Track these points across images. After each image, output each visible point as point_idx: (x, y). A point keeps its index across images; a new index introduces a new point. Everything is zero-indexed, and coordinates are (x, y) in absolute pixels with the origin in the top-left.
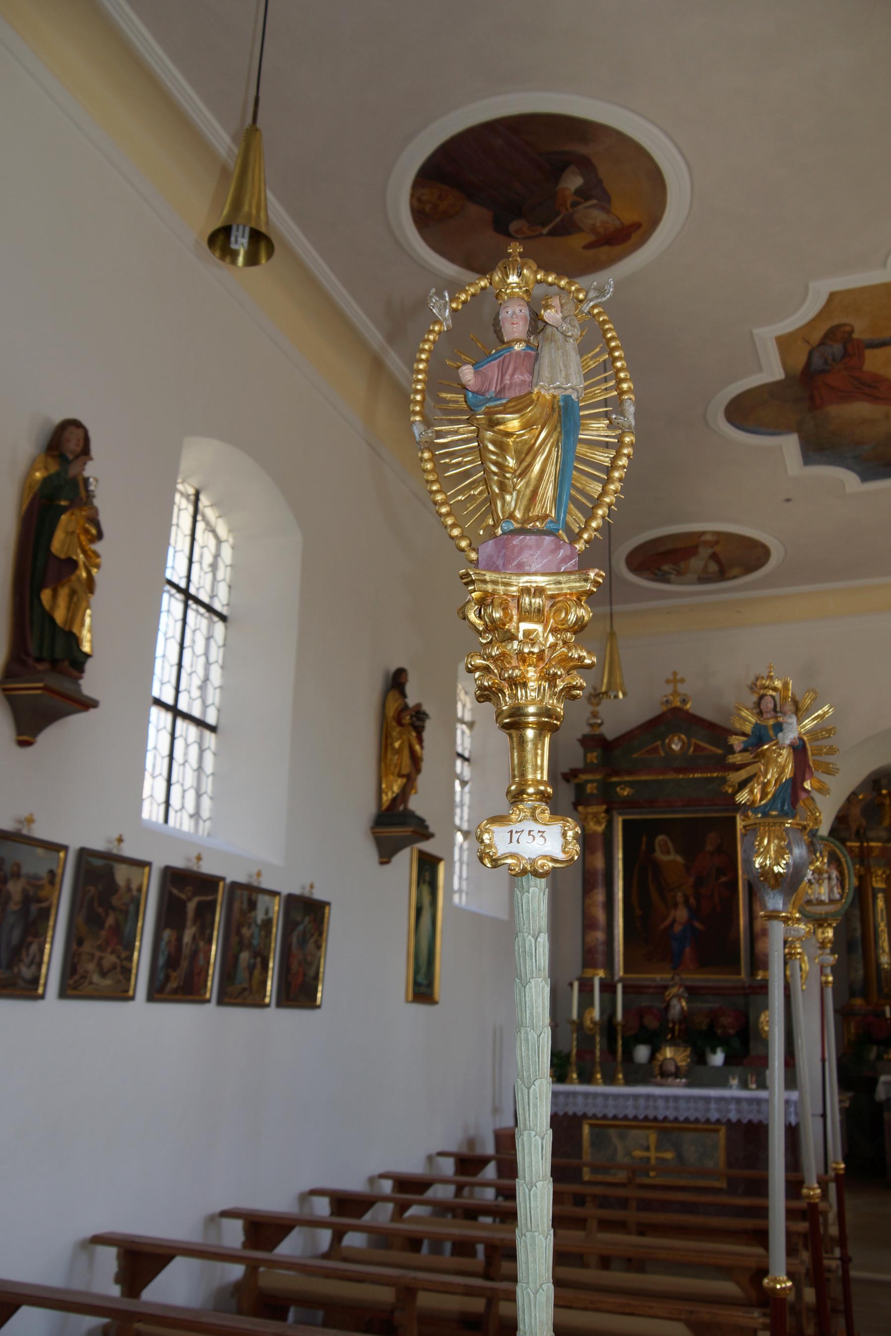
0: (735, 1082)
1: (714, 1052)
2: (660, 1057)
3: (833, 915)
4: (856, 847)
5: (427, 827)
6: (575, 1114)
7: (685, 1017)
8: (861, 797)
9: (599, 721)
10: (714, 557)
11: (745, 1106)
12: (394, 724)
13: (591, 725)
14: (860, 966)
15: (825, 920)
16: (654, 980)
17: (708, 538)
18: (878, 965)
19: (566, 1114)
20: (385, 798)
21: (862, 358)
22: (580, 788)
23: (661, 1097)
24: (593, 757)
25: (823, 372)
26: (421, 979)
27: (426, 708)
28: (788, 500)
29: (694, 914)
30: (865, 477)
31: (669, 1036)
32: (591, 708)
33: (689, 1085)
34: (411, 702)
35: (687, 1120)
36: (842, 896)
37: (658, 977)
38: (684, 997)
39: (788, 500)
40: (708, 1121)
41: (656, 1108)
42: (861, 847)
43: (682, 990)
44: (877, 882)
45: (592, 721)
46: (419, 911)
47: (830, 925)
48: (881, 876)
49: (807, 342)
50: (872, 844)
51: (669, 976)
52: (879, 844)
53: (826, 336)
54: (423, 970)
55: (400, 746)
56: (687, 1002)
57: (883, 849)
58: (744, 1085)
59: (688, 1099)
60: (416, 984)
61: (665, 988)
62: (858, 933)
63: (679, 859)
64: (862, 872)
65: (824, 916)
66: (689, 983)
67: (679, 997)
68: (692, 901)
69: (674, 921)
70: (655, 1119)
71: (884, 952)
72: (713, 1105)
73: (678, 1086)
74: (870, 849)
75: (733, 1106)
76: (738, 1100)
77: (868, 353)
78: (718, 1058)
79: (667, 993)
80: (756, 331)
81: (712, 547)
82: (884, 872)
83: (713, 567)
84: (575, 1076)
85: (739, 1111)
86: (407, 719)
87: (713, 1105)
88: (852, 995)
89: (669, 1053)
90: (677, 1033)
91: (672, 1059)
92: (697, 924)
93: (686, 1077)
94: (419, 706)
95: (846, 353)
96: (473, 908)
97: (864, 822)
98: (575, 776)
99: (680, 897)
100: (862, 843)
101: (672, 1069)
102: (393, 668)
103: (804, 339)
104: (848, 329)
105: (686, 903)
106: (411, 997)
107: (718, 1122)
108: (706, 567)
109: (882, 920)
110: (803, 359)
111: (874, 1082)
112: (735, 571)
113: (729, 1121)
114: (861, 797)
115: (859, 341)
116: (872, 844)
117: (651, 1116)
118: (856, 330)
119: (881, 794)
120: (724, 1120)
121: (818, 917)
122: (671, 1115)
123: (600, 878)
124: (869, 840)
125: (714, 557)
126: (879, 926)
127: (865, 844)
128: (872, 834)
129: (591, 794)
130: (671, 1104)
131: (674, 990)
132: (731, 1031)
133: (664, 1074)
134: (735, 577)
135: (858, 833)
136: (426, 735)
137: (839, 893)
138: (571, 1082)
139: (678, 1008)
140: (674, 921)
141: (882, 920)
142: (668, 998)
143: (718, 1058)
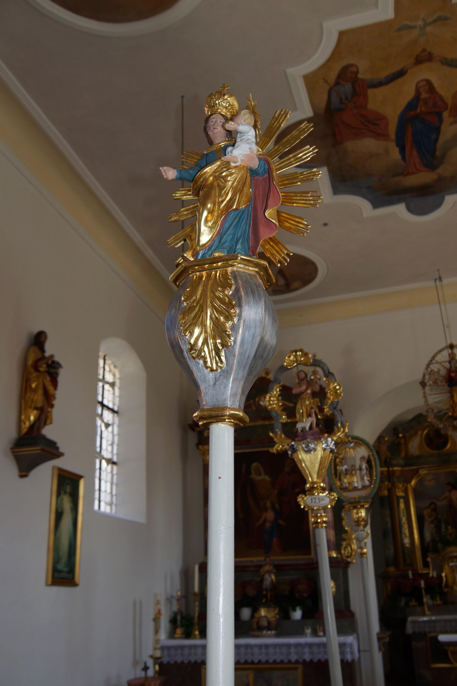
0: (309, 631)
1: (295, 610)
2: (257, 615)
3: (365, 499)
4: (385, 471)
5: (57, 448)
6: (196, 661)
7: (274, 586)
8: (386, 439)
11: (315, 649)
12: (32, 370)
15: (359, 502)
16: (252, 561)
18: (403, 545)
19: (190, 662)
20: (23, 426)
23: (256, 646)
27: (56, 359)
28: (325, 225)
30: (376, 205)
31: (264, 600)
33: (278, 635)
34: (47, 354)
35: (275, 662)
36: (371, 483)
37: (255, 559)
38: (273, 573)
39: (325, 225)
40: (290, 662)
41: (252, 654)
42: (388, 471)
43: (271, 567)
44: (399, 492)
46: (59, 515)
47: (362, 507)
49: (326, 82)
50: (395, 468)
51: (262, 558)
52: (399, 468)
54: (64, 559)
55: (37, 386)
56: (276, 576)
58: (315, 633)
59: (275, 646)
61: (260, 566)
62: (389, 525)
64: (390, 486)
65: (357, 500)
66: (276, 563)
67: (269, 572)
70: (252, 662)
71: (406, 536)
72: (293, 650)
73: (269, 636)
74: (394, 472)
75: (307, 650)
76: (310, 645)
77: (371, 92)
78: (297, 614)
79: (261, 570)
80: (288, 71)
82: (403, 486)
84: (197, 633)
85: (311, 653)
86: (43, 368)
87: (293, 650)
89: (263, 612)
90: (269, 598)
91: (265, 617)
93: (275, 629)
94: (52, 356)
96: (121, 515)
100: (388, 467)
101: (265, 623)
102: (36, 330)
103: (323, 79)
106: (50, 582)
107: (297, 662)
109: (404, 516)
110: (325, 97)
111: (404, 621)
113: (304, 661)
114: (386, 439)
116: (395, 468)
117: (249, 661)
118: (361, 70)
120: (301, 661)
121: (353, 500)
122: (263, 658)
124: (393, 466)
128: (394, 462)
130: (264, 650)
131: (267, 568)
132: (305, 595)
133: (260, 628)
136: (60, 379)
137: (368, 481)
138: (195, 638)
139: (269, 580)
141: (404, 516)
142: (262, 574)
143: (297, 614)
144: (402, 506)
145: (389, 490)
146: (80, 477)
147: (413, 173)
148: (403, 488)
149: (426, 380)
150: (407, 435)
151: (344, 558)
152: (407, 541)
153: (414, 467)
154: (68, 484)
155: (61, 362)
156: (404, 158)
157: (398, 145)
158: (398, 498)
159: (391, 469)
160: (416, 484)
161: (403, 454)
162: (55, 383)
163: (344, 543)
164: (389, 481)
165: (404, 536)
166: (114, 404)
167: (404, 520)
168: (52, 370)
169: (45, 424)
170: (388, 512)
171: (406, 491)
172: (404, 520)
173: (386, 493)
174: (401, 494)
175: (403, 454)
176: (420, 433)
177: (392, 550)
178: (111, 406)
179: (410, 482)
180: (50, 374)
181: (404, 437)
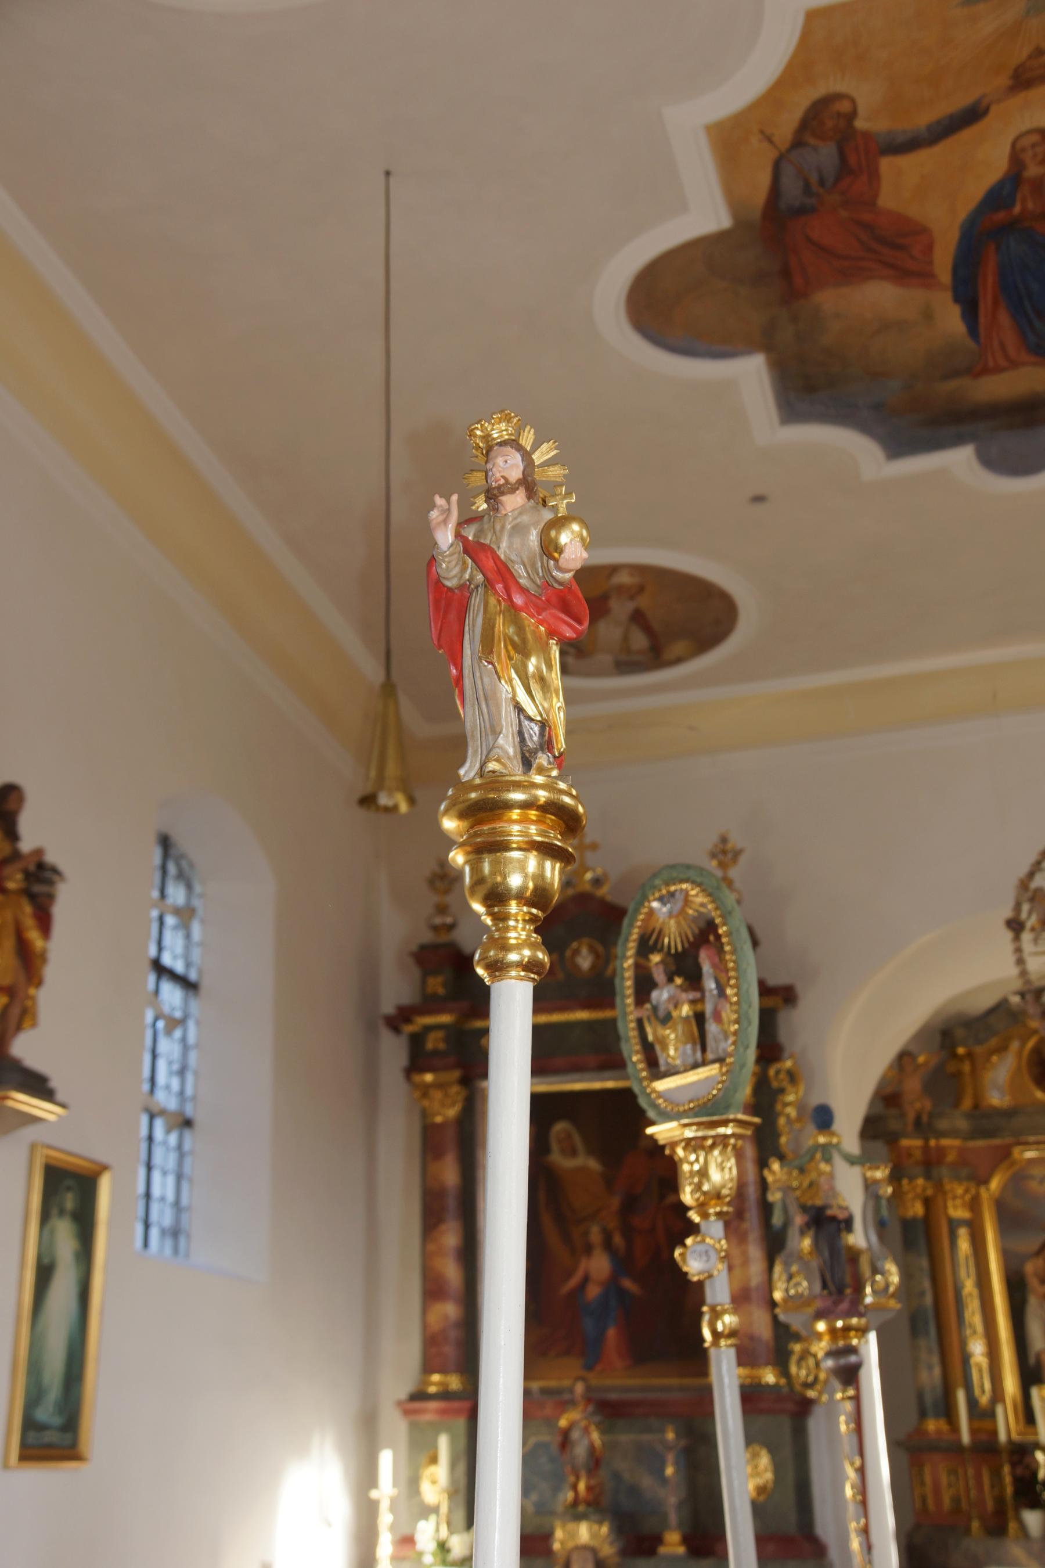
8: (921, 1059)
9: (449, 920)
10: (638, 618)
13: (436, 929)
14: (935, 1360)
17: (624, 578)
21: (874, 176)
22: (416, 1041)
24: (437, 984)
25: (801, 211)
26: (45, 1414)
27: (51, 857)
29: (623, 1264)
32: (434, 899)
34: (26, 845)
42: (926, 1148)
45: (438, 921)
46: (44, 1273)
48: (962, 1197)
49: (769, 139)
52: (956, 1143)
53: (804, 125)
57: (962, 1151)
60: (29, 1424)
62: (928, 1300)
63: (593, 1164)
64: (930, 1192)
66: (614, 1396)
68: (618, 1240)
69: (586, 1279)
71: (975, 1332)
74: (941, 1151)
77: (887, 165)
81: (632, 597)
82: (967, 1191)
83: (639, 640)
88: (923, 1414)
92: (628, 1284)
94: (39, 852)
95: (845, 169)
97: (928, 1104)
98: (408, 1020)
99: (595, 1234)
103: (762, 132)
104: (844, 106)
105: (608, 1245)
108: (626, 639)
109: (968, 1276)
110: (764, 180)
112: (679, 648)
114: (921, 1059)
115: (867, 135)
116: (945, 1142)
118: (862, 111)
119: (954, 1055)
123: (452, 1203)
125: (638, 618)
126: (963, 1287)
127: (933, 1143)
128: (943, 1124)
129: (436, 1053)
134: (679, 661)
135: (918, 1122)
140: (586, 1279)
141: (968, 1276)
144: (964, 1245)
145: (927, 1202)
146: (105, 1168)
147: (998, 370)
148: (968, 1197)
149: (1024, 915)
150: (979, 1050)
151: (798, 1388)
152: (977, 1349)
153: (997, 1141)
154: (69, 1189)
155: (62, 866)
156: (973, 329)
157: (957, 300)
158: (953, 1225)
159: (933, 1143)
160: (1004, 1188)
161: (967, 1103)
162: (44, 922)
163: (797, 1348)
164: (928, 1177)
165: (968, 1332)
166: (188, 965)
167: (969, 1286)
168: (38, 888)
169: (19, 1028)
170: (924, 1263)
171: (974, 1205)
172: (969, 1286)
173: (918, 1209)
174: (958, 1212)
175: (967, 1103)
176: (1015, 1045)
177: (937, 1371)
178: (179, 967)
179: (986, 1181)
180: (32, 897)
181: (970, 1055)
